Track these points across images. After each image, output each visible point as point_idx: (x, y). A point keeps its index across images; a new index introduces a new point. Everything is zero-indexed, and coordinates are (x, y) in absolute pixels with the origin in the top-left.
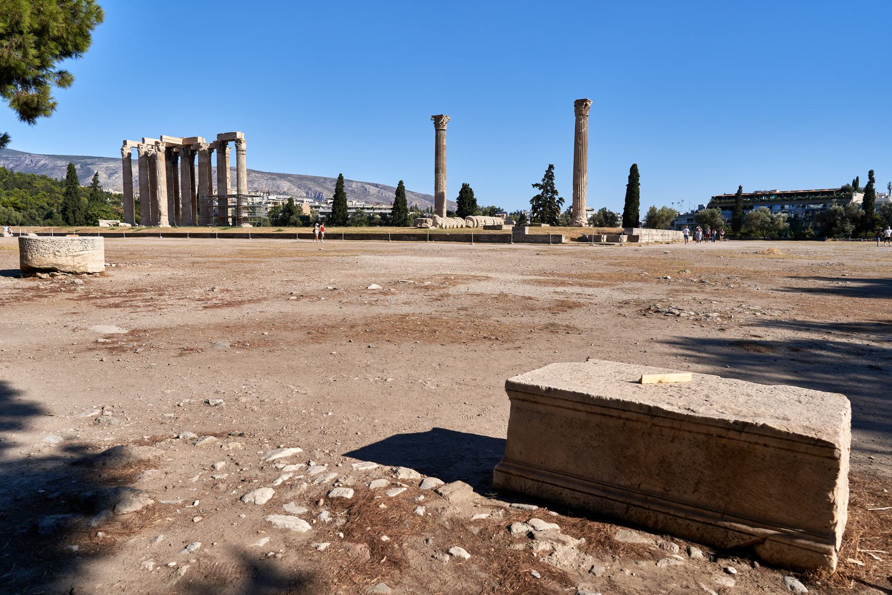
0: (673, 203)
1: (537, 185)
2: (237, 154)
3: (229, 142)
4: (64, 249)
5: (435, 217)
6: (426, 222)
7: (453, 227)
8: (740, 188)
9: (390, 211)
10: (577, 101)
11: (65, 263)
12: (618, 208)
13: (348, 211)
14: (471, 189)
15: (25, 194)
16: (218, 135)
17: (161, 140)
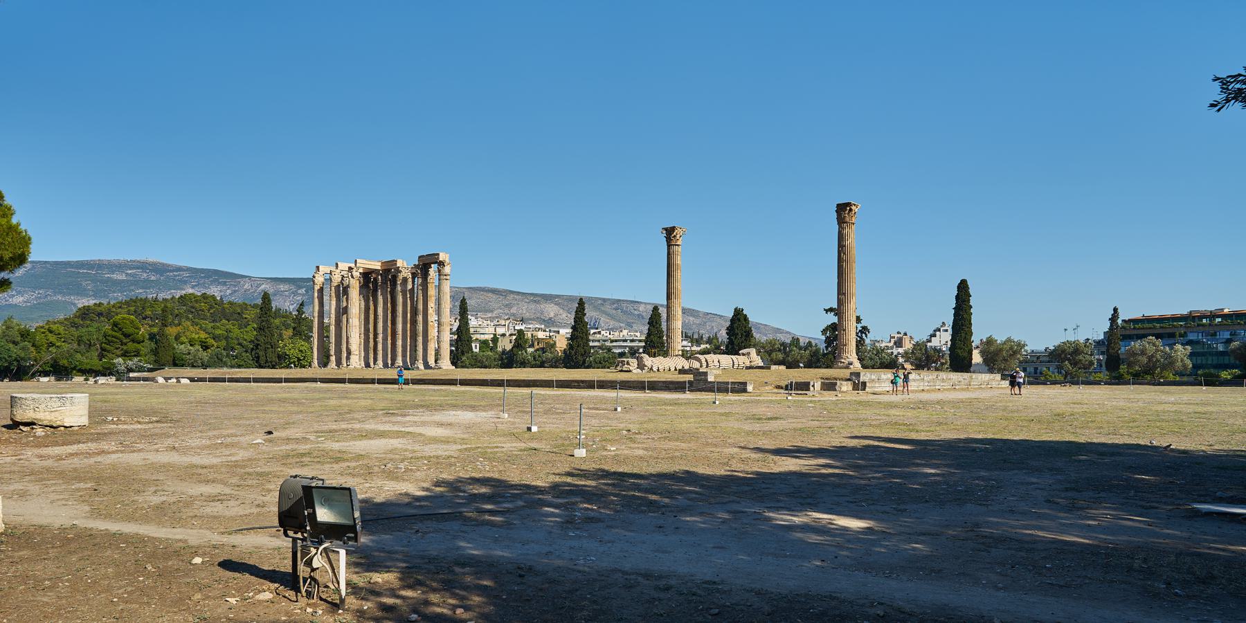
0: (1066, 330)
1: (831, 310)
2: (439, 280)
3: (432, 265)
4: (43, 406)
5: (642, 357)
6: (628, 363)
7: (670, 370)
8: (1115, 310)
9: (643, 344)
10: (838, 205)
11: (43, 418)
12: (943, 340)
13: (591, 344)
14: (746, 315)
15: (232, 327)
16: (420, 257)
17: (356, 265)
